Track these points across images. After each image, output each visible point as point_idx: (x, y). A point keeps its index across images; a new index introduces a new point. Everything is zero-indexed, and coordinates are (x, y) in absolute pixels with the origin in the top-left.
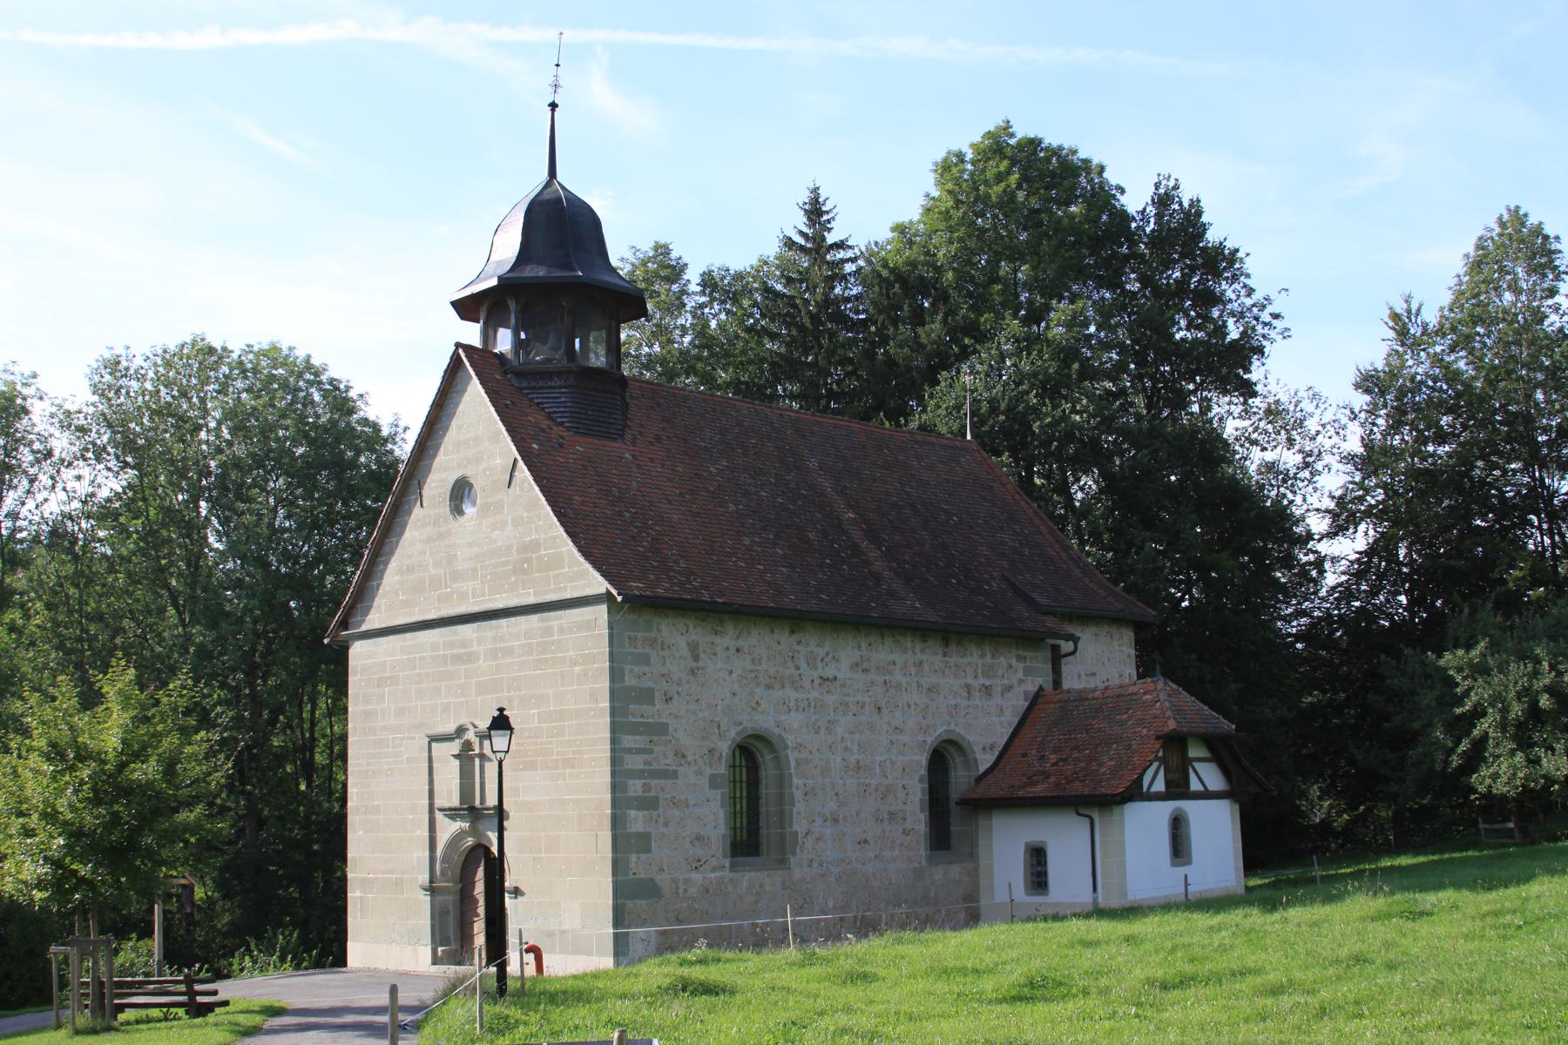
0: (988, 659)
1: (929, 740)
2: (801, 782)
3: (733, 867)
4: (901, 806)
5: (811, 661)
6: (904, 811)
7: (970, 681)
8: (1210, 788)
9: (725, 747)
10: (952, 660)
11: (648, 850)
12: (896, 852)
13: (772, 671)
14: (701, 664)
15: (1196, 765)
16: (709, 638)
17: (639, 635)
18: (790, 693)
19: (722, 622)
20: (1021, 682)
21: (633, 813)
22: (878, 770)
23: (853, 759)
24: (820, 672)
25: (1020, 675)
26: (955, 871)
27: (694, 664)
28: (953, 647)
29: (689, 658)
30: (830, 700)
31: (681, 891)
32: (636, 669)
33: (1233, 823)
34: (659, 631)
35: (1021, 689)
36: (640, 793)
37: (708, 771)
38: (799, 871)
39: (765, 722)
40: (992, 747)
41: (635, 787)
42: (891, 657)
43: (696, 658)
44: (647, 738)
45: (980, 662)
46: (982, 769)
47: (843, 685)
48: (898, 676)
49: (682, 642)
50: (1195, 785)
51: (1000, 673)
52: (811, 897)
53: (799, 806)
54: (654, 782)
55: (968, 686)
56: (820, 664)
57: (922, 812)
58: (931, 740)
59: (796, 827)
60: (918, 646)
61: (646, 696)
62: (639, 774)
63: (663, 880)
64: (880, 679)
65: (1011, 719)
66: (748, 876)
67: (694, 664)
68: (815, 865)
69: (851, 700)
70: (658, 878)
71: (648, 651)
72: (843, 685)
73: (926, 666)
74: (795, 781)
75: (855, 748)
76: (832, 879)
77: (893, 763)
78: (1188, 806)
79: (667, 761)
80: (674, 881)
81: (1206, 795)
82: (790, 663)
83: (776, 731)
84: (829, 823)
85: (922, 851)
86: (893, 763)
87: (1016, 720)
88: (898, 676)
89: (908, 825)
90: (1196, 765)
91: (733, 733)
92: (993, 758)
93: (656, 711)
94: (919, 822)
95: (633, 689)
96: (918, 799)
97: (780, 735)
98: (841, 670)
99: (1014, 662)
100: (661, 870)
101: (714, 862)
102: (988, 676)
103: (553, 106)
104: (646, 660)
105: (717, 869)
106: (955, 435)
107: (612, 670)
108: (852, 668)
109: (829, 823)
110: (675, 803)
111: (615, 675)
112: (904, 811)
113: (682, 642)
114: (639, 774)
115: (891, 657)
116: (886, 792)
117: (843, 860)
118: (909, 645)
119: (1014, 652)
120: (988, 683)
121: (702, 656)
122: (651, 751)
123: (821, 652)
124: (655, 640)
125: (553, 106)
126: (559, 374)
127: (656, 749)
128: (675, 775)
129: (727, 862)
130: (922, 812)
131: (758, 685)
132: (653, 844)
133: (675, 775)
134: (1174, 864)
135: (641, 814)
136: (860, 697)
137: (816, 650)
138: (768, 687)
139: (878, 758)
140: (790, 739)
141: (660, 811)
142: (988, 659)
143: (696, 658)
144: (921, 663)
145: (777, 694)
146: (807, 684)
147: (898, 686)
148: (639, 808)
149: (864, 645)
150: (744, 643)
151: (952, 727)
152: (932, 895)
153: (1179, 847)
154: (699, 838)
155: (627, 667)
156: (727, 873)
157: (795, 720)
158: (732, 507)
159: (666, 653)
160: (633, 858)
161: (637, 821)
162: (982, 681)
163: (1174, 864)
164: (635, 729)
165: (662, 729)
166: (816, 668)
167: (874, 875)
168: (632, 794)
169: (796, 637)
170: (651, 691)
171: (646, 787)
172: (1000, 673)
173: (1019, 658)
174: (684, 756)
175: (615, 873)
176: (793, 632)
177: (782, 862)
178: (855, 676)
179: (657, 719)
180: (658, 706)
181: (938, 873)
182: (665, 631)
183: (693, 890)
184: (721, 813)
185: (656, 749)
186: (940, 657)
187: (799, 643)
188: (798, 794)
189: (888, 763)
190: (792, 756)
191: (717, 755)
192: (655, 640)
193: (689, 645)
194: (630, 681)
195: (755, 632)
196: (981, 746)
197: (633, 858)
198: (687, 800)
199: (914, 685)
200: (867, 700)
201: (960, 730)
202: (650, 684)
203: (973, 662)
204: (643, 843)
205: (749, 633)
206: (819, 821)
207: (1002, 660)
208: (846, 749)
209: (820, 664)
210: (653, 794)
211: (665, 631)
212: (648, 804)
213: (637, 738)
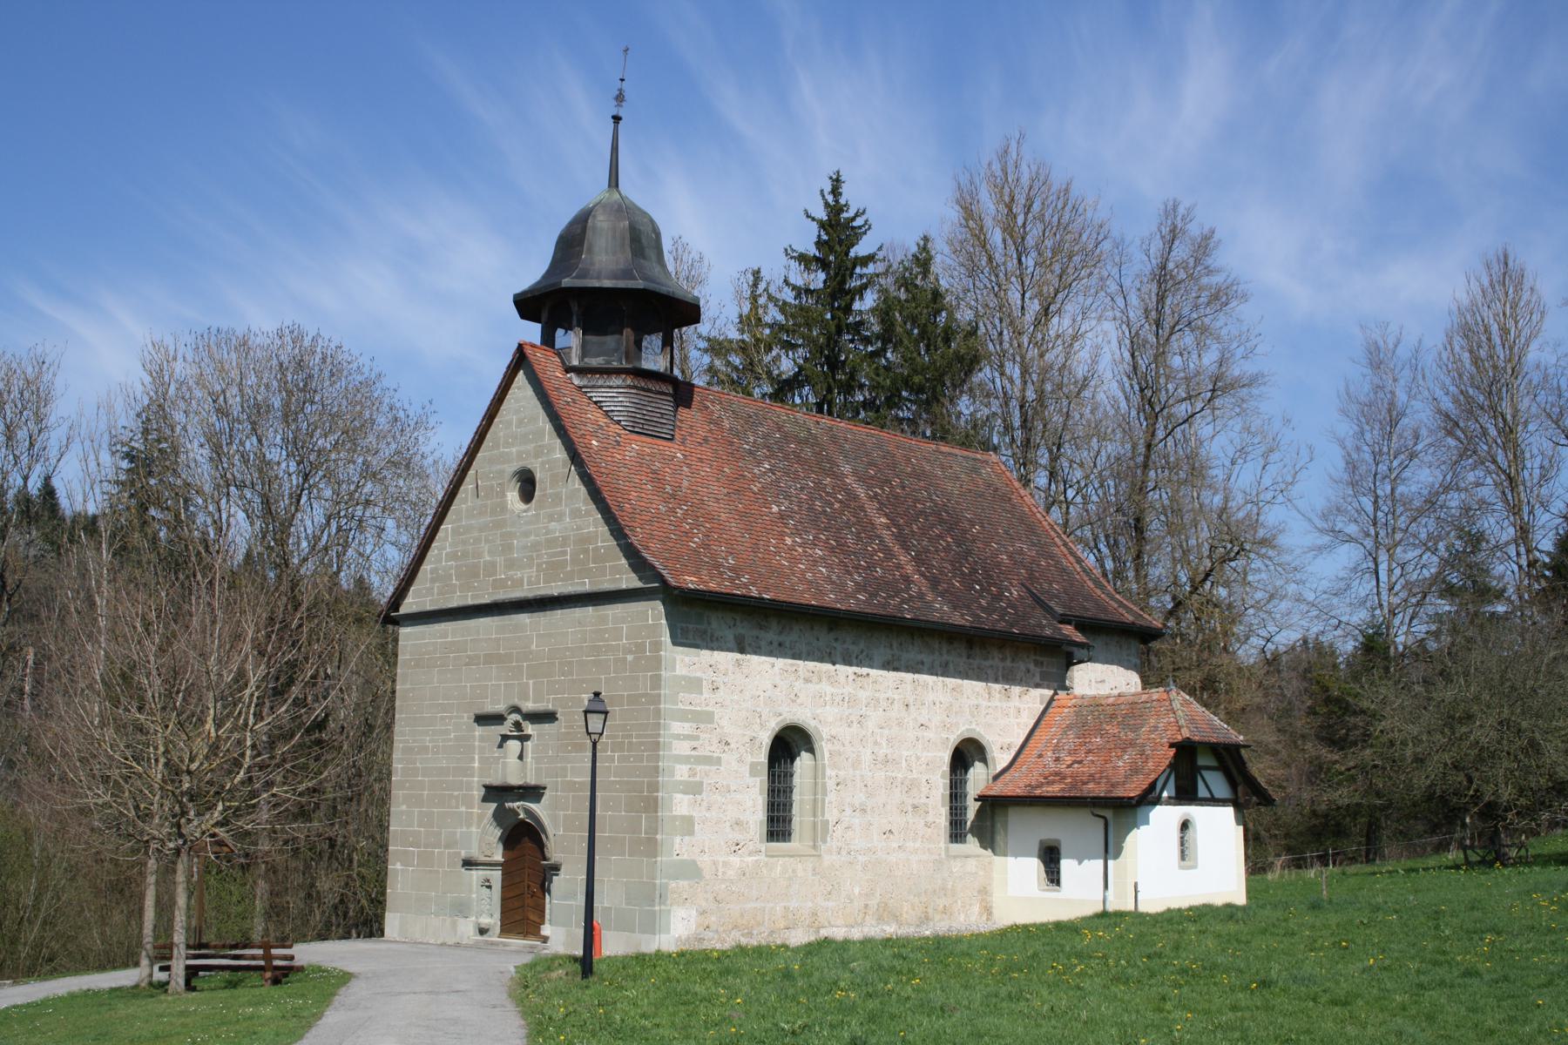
0: (1008, 663)
4: (924, 800)
8: (1217, 795)
11: (691, 833)
12: (918, 845)
16: (755, 632)
17: (691, 626)
21: (678, 796)
22: (904, 764)
31: (720, 874)
32: (687, 659)
34: (709, 623)
36: (685, 778)
44: (695, 726)
45: (1001, 665)
50: (1202, 792)
54: (699, 768)
57: (943, 806)
58: (954, 739)
59: (827, 816)
62: (686, 759)
63: (704, 861)
68: (844, 853)
69: (882, 696)
73: (951, 666)
74: (828, 772)
77: (918, 758)
81: (1213, 801)
86: (918, 758)
89: (930, 819)
90: (1205, 773)
95: (684, 678)
99: (1032, 666)
101: (751, 846)
103: (617, 119)
109: (857, 814)
114: (686, 759)
115: (920, 657)
116: (911, 787)
118: (937, 646)
122: (697, 738)
125: (617, 119)
127: (702, 736)
130: (943, 806)
133: (718, 761)
135: (686, 797)
136: (889, 694)
137: (852, 647)
138: (807, 681)
139: (905, 753)
144: (947, 664)
148: (685, 793)
151: (973, 726)
152: (949, 887)
156: (762, 857)
158: (775, 509)
168: (678, 778)
170: (699, 681)
171: (693, 773)
173: (1037, 663)
174: (727, 744)
180: (706, 695)
182: (714, 625)
183: (731, 873)
186: (964, 659)
187: (836, 640)
188: (831, 784)
191: (757, 743)
192: (705, 632)
193: (735, 637)
197: (678, 840)
198: (728, 786)
200: (896, 697)
202: (699, 674)
205: (791, 629)
206: (848, 811)
207: (1022, 666)
208: (876, 743)
211: (714, 625)
213: (687, 725)
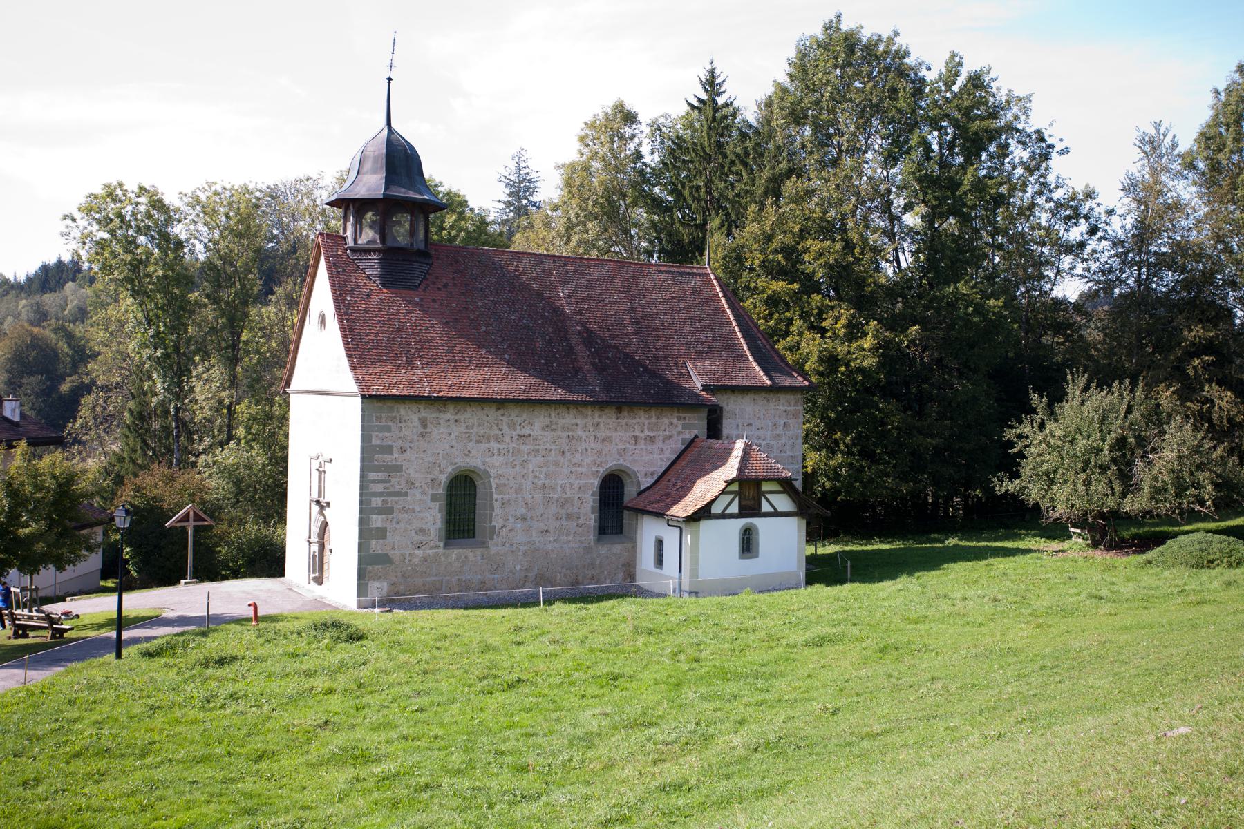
0: (654, 420)
1: (601, 470)
2: (499, 497)
3: (446, 546)
4: (576, 510)
5: (512, 426)
6: (579, 513)
7: (637, 433)
8: (780, 509)
9: (444, 478)
10: (623, 422)
11: (384, 537)
12: (570, 538)
13: (482, 432)
14: (428, 430)
15: (768, 496)
16: (435, 415)
17: (383, 415)
18: (494, 445)
19: (445, 405)
20: (679, 433)
21: (374, 517)
22: (559, 489)
23: (540, 483)
24: (518, 432)
25: (680, 428)
26: (617, 548)
27: (423, 430)
28: (625, 413)
29: (420, 426)
30: (525, 448)
31: (407, 561)
32: (381, 435)
33: (799, 531)
34: (398, 412)
35: (680, 438)
36: (380, 505)
37: (430, 492)
38: (495, 547)
39: (475, 462)
40: (652, 474)
41: (377, 502)
42: (574, 421)
43: (425, 427)
44: (387, 474)
45: (646, 422)
46: (643, 487)
47: (536, 439)
48: (579, 432)
49: (415, 418)
50: (765, 507)
51: (663, 428)
52: (503, 564)
53: (498, 511)
54: (390, 499)
55: (636, 438)
56: (518, 427)
57: (592, 513)
58: (602, 471)
59: (494, 523)
60: (597, 413)
61: (388, 450)
62: (380, 494)
63: (396, 555)
64: (565, 434)
65: (669, 456)
66: (456, 551)
67: (423, 430)
68: (508, 545)
69: (540, 448)
70: (391, 553)
71: (390, 423)
72: (536, 439)
73: (602, 425)
74: (495, 496)
75: (542, 476)
76: (520, 553)
77: (571, 485)
78: (756, 521)
79: (403, 487)
80: (403, 555)
81: (776, 514)
82: (495, 427)
83: (482, 467)
84: (519, 521)
85: (592, 537)
86: (571, 485)
87: (674, 457)
88: (579, 432)
89: (581, 521)
90: (768, 496)
91: (450, 469)
92: (653, 480)
93: (395, 458)
94: (591, 520)
95: (377, 446)
96: (590, 506)
97: (485, 470)
98: (536, 430)
99: (675, 421)
100: (393, 548)
101: (432, 544)
102: (652, 430)
103: (390, 79)
104: (388, 429)
105: (434, 546)
106: (272, 395)
107: (363, 436)
108: (543, 429)
109: (519, 521)
110: (405, 511)
111: (365, 438)
112: (579, 513)
113: (415, 418)
114: (380, 494)
115: (574, 421)
116: (565, 502)
117: (529, 542)
118: (590, 413)
119: (676, 414)
120: (652, 435)
121: (429, 425)
122: (389, 481)
123: (519, 420)
124: (395, 417)
125: (390, 79)
126: (374, 251)
127: (393, 480)
128: (406, 494)
129: (442, 544)
130: (592, 513)
131: (470, 441)
132: (388, 534)
133: (406, 494)
134: (741, 557)
135: (380, 517)
136: (548, 446)
137: (516, 419)
138: (477, 442)
139: (560, 482)
140: (492, 472)
141: (394, 515)
142: (654, 420)
143: (425, 427)
144: (598, 424)
145: (484, 446)
146: (507, 439)
147: (579, 439)
148: (379, 514)
149: (553, 415)
150: (461, 417)
151: (621, 462)
152: (598, 562)
153: (748, 544)
154: (421, 530)
155: (374, 434)
156: (441, 550)
157: (497, 460)
158: (483, 329)
159: (403, 425)
160: (374, 542)
161: (377, 521)
162: (647, 433)
163: (741, 557)
164: (378, 469)
165: (398, 468)
166: (515, 429)
167: (552, 551)
168: (374, 505)
169: (500, 412)
170: (391, 447)
171: (384, 502)
172: (663, 428)
173: (679, 418)
174: (413, 483)
175: (360, 550)
176: (499, 409)
177: (483, 544)
178: (546, 433)
179: (394, 463)
180: (395, 455)
181: (604, 550)
182: (402, 412)
183: (416, 560)
184: (439, 516)
185: (393, 480)
186: (614, 420)
187: (503, 415)
188: (496, 504)
189: (567, 485)
190: (494, 483)
191: (437, 482)
192: (395, 417)
193: (419, 419)
194: (375, 441)
195: (469, 410)
196: (643, 473)
197: (374, 542)
198: (414, 509)
199: (592, 438)
200: (554, 447)
201: (626, 463)
202: (390, 443)
203: (641, 422)
204: (382, 533)
205: (465, 411)
206: (512, 520)
207: (666, 421)
208: (536, 477)
209: (518, 427)
210: (389, 505)
211: (402, 412)
212: (386, 511)
213: (380, 474)
